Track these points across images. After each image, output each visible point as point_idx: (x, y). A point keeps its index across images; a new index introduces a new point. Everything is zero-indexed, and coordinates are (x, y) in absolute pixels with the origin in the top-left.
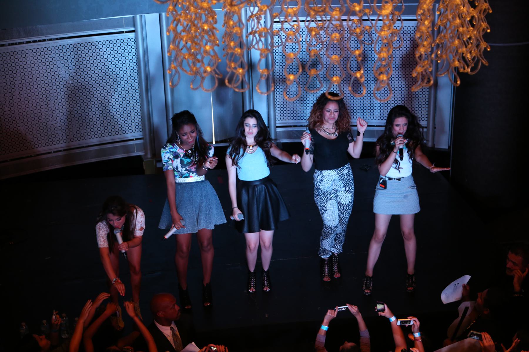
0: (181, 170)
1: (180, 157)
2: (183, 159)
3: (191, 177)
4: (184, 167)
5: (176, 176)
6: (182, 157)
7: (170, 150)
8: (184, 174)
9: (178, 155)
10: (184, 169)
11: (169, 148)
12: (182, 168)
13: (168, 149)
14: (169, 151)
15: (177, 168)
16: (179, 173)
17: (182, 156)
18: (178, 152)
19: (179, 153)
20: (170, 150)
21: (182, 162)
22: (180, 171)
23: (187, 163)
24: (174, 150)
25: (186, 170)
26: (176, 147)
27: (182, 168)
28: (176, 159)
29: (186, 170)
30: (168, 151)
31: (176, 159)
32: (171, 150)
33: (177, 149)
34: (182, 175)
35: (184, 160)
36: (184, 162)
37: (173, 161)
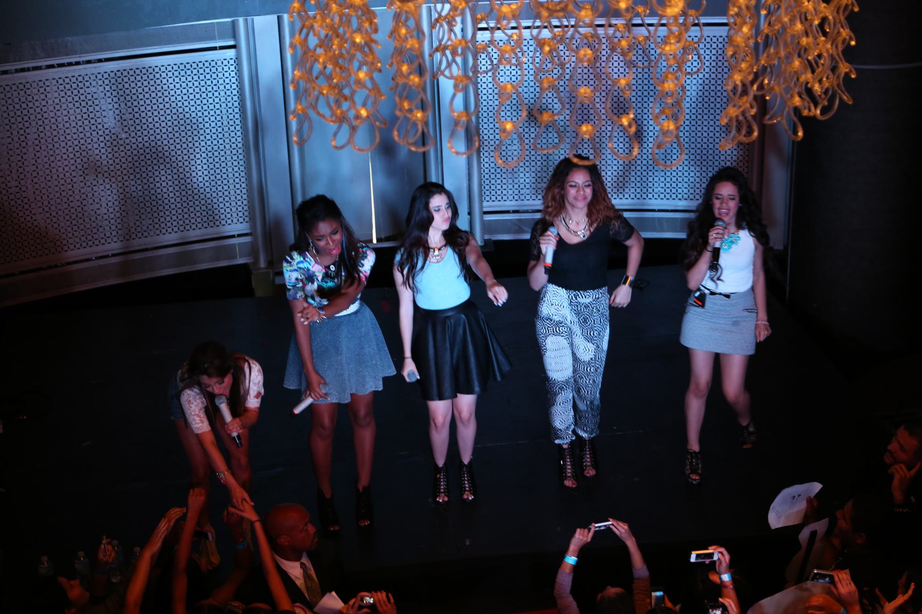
1: (317, 279)
2: (321, 284)
11: (296, 261)
13: (295, 264)
14: (298, 267)
17: (320, 278)
19: (314, 272)
20: (299, 266)
26: (309, 260)
30: (296, 268)
31: (310, 284)
32: (301, 265)
33: (310, 264)
37: (304, 285)
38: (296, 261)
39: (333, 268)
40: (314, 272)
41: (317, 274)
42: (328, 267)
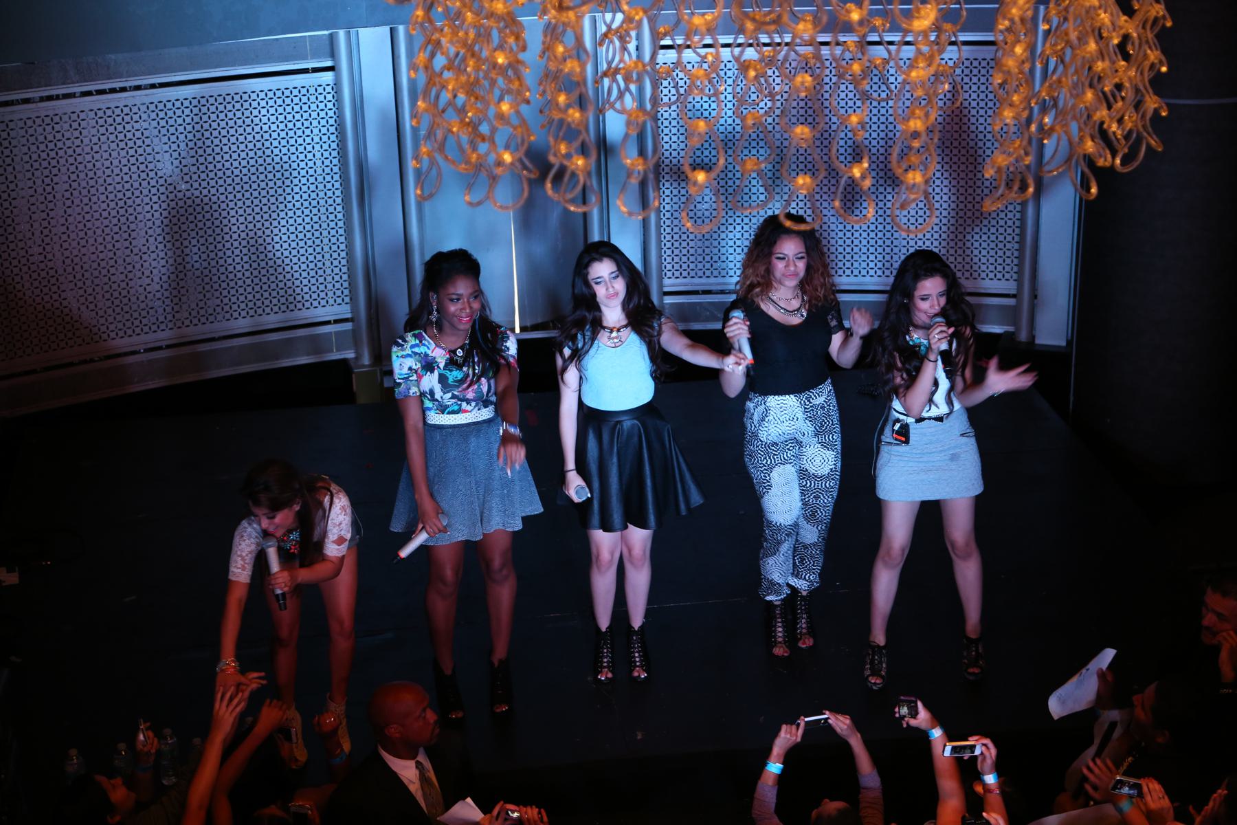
1: (438, 367)
2: (444, 372)
3: (466, 411)
4: (448, 392)
5: (430, 409)
7: (413, 350)
8: (447, 407)
9: (432, 363)
10: (449, 395)
11: (410, 344)
13: (409, 346)
14: (412, 352)
15: (432, 392)
16: (436, 403)
17: (442, 366)
18: (433, 355)
19: (435, 358)
20: (413, 350)
21: (442, 379)
22: (440, 399)
23: (455, 381)
24: (422, 349)
25: (454, 397)
26: (426, 343)
27: (444, 393)
28: (429, 373)
29: (454, 397)
30: (410, 353)
31: (429, 373)
32: (416, 350)
33: (429, 349)
34: (443, 409)
35: (448, 373)
36: (447, 378)
37: (420, 377)
38: (410, 344)
39: (460, 353)
40: (435, 358)
41: (438, 360)
42: (454, 352)
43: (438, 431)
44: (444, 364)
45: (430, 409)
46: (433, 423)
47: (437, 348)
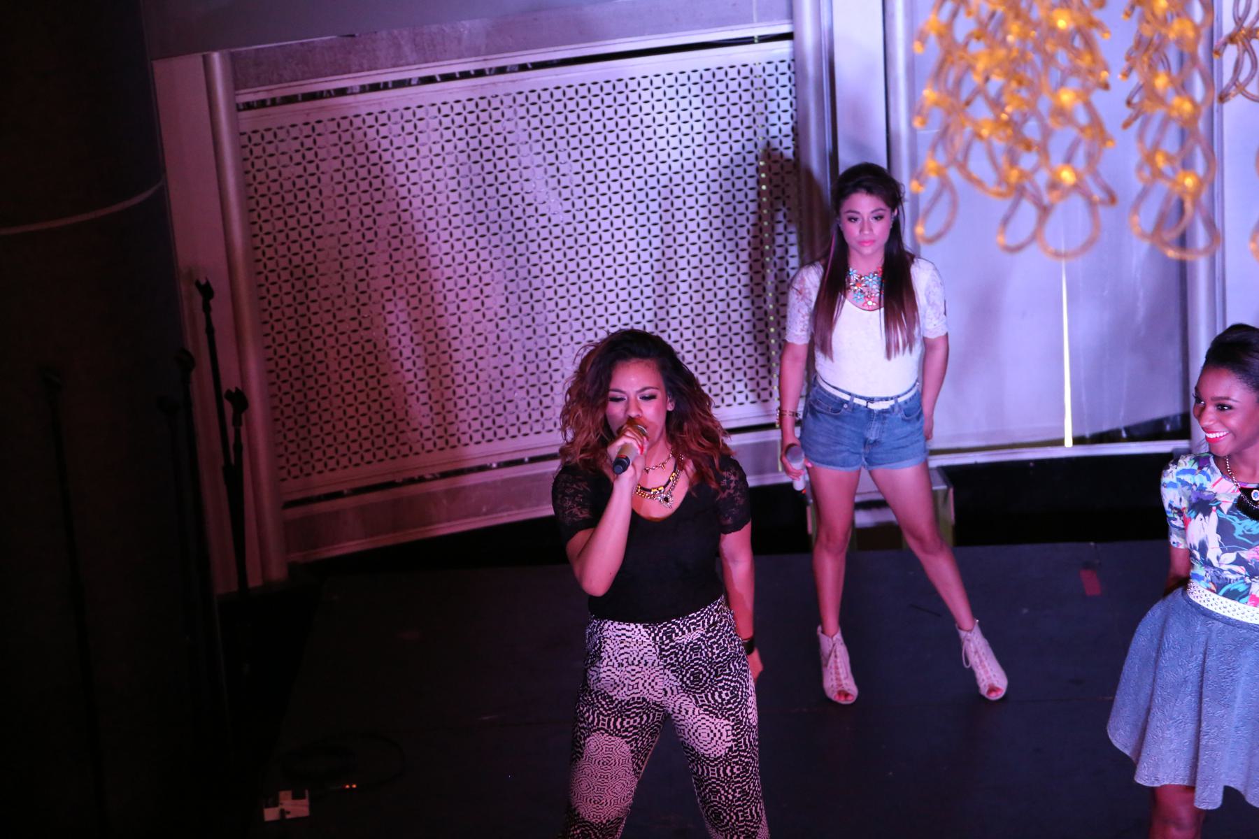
0: (1218, 558)
1: (1218, 507)
2: (1228, 518)
4: (1231, 551)
5: (1199, 578)
6: (1225, 512)
7: (1182, 477)
9: (1208, 502)
10: (1231, 557)
11: (1179, 468)
12: (1224, 551)
13: (1175, 471)
14: (1179, 480)
15: (1203, 548)
16: (1211, 571)
17: (1226, 507)
18: (1214, 490)
19: (1215, 494)
20: (1182, 477)
21: (1224, 529)
22: (1215, 563)
23: (1245, 535)
24: (1199, 479)
25: (1239, 561)
26: (1209, 472)
27: (1224, 551)
28: (1200, 516)
29: (1239, 561)
30: (1175, 480)
31: (1200, 516)
32: (1188, 478)
33: (1209, 479)
36: (1233, 528)
37: (1186, 522)
38: (1179, 468)
40: (1215, 494)
41: (1221, 498)
43: (1203, 618)
44: (1229, 505)
45: (1199, 578)
46: (1197, 601)
47: (1224, 480)
